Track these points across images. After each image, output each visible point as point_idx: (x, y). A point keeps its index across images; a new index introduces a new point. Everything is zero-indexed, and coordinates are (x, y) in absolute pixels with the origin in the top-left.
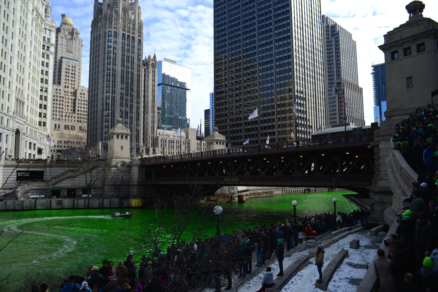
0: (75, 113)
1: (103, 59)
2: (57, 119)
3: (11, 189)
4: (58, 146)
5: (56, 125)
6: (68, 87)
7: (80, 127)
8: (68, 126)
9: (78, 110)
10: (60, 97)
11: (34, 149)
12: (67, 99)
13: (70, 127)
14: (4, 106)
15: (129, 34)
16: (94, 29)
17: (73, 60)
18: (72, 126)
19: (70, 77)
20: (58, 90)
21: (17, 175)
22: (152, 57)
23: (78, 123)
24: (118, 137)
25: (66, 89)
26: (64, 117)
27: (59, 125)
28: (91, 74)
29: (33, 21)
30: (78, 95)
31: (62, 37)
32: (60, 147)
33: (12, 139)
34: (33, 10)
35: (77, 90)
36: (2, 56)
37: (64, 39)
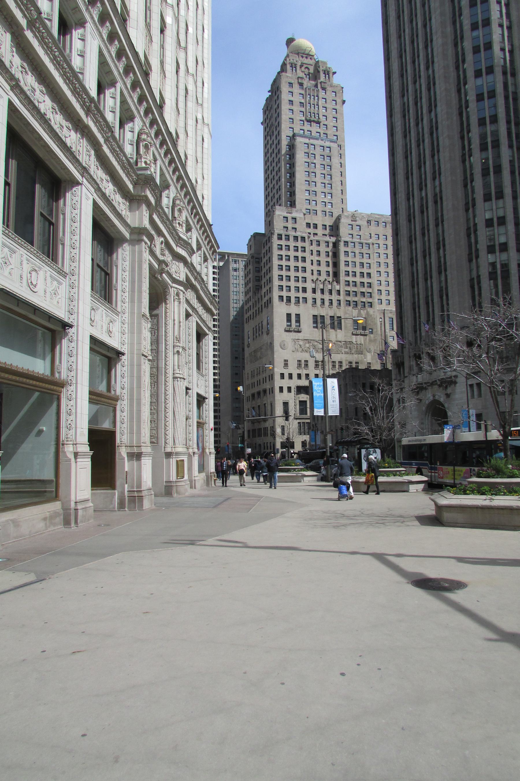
0: (338, 282)
4: (299, 376)
8: (323, 317)
9: (347, 274)
10: (296, 238)
12: (314, 243)
13: (328, 321)
18: (332, 317)
20: (290, 219)
23: (350, 308)
26: (309, 295)
27: (298, 316)
30: (344, 231)
31: (291, 84)
32: (303, 377)
35: (338, 219)
37: (296, 89)
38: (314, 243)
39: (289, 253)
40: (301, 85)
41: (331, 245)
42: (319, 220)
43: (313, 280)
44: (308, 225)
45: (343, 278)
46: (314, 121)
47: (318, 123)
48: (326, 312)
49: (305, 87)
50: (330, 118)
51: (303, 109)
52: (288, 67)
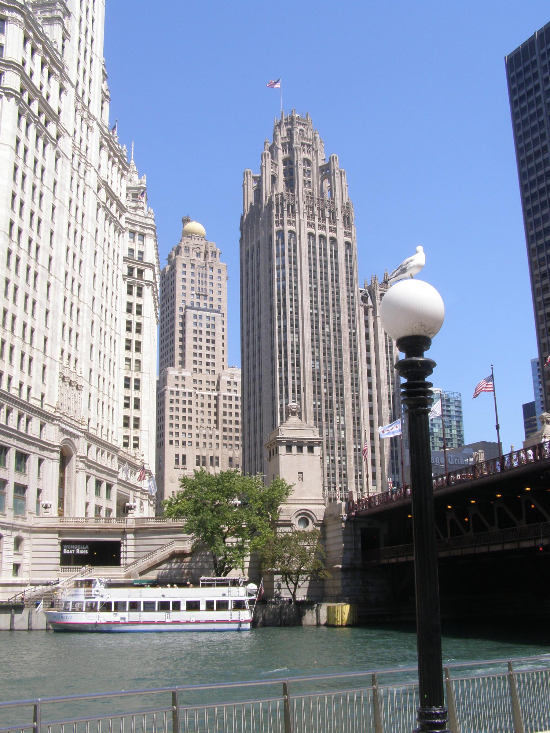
0: (217, 428)
1: (268, 295)
2: (181, 443)
3: (47, 584)
5: (177, 456)
6: (201, 370)
7: (231, 459)
8: (204, 457)
10: (184, 393)
11: (108, 496)
12: (199, 396)
14: (32, 391)
15: (323, 233)
16: (247, 232)
17: (208, 311)
18: (212, 458)
19: (204, 348)
20: (180, 378)
21: (62, 552)
22: (380, 280)
24: (289, 449)
25: (198, 376)
26: (194, 439)
27: (184, 457)
28: (245, 332)
29: (101, 210)
30: (224, 386)
31: (184, 265)
33: (52, 468)
34: (99, 189)
36: (8, 264)
37: (189, 270)
38: (199, 396)
39: (179, 406)
40: (193, 265)
41: (213, 398)
42: (204, 377)
43: (197, 427)
44: (195, 381)
45: (221, 425)
46: (202, 295)
47: (206, 296)
48: (207, 453)
49: (196, 266)
50: (215, 291)
51: (193, 285)
52: (183, 249)
